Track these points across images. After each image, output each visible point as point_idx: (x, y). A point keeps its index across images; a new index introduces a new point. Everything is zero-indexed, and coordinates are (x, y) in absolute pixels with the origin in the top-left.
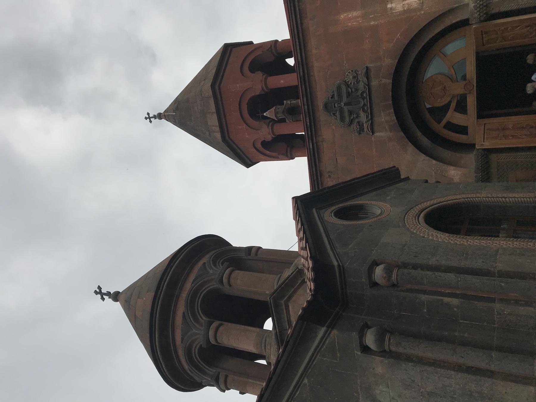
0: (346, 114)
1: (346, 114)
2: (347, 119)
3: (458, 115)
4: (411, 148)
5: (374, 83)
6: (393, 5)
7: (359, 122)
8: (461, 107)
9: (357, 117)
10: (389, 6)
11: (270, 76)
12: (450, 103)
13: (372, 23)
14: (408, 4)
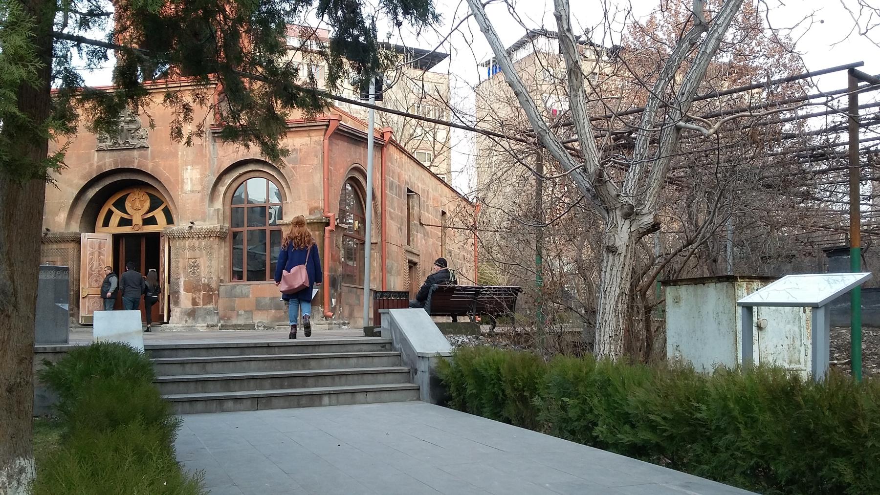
4: (83, 183)
5: (136, 153)
8: (124, 222)
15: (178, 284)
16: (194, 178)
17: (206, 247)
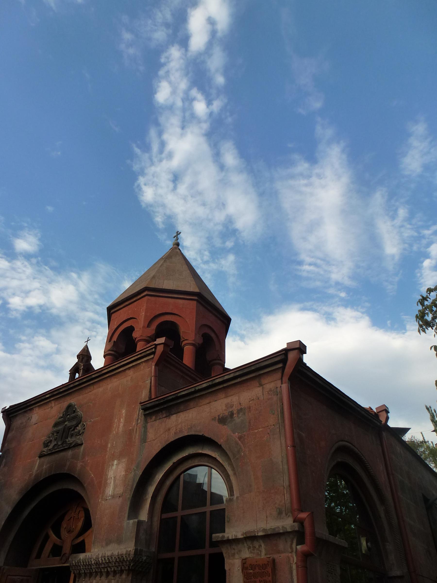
0: (60, 427)
2: (55, 429)
3: (51, 546)
5: (70, 453)
7: (51, 441)
9: (55, 439)
13: (109, 446)
14: (110, 483)
16: (118, 477)
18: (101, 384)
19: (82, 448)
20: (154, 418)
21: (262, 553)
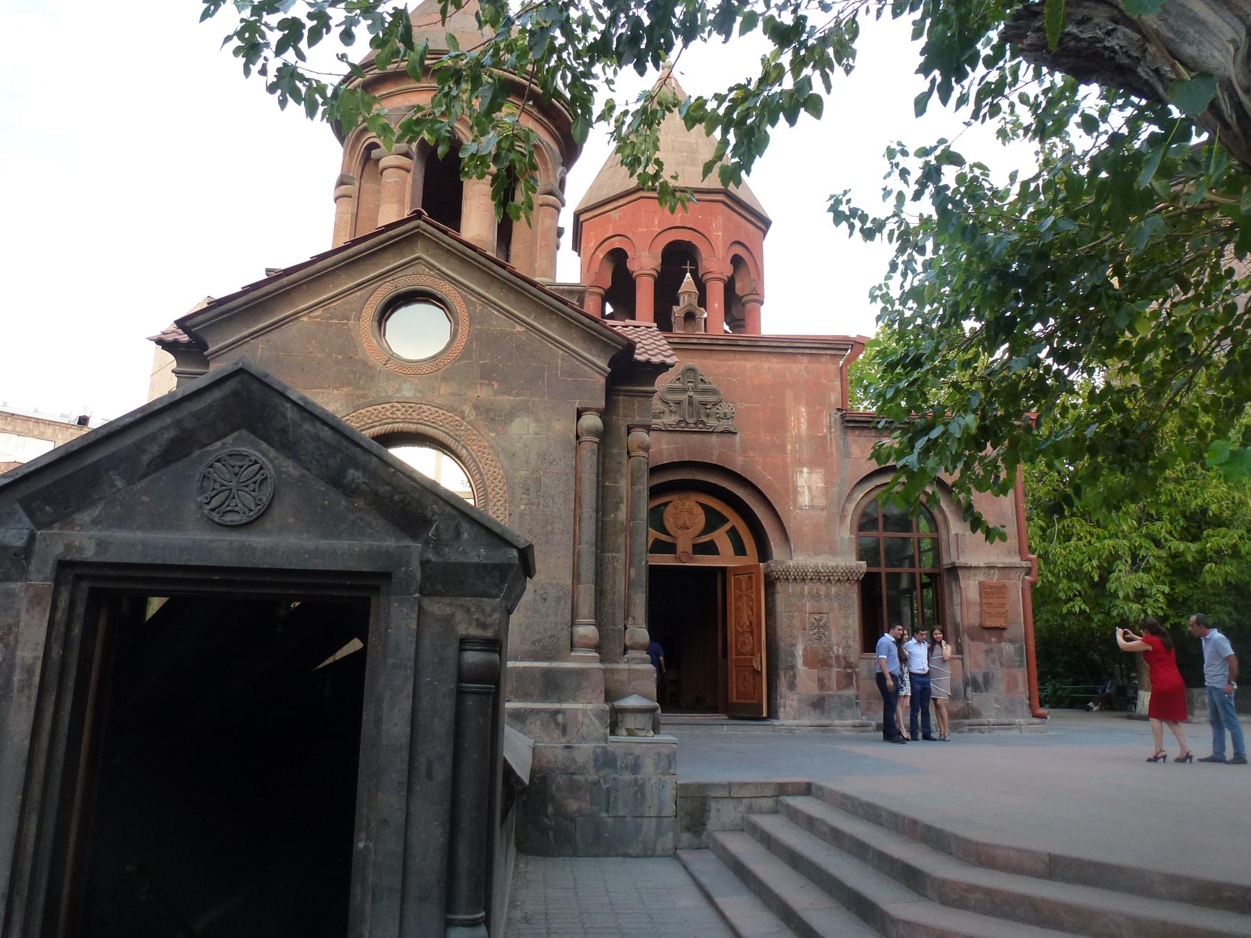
0: (677, 397)
1: (677, 397)
2: (669, 397)
6: (805, 475)
10: (805, 470)
11: (725, 287)
12: (669, 534)
13: (789, 447)
15: (793, 655)
16: (814, 487)
17: (837, 594)
18: (749, 356)
19: (738, 437)
20: (857, 432)
21: (995, 578)
